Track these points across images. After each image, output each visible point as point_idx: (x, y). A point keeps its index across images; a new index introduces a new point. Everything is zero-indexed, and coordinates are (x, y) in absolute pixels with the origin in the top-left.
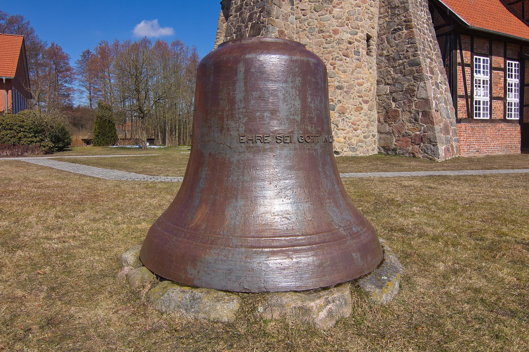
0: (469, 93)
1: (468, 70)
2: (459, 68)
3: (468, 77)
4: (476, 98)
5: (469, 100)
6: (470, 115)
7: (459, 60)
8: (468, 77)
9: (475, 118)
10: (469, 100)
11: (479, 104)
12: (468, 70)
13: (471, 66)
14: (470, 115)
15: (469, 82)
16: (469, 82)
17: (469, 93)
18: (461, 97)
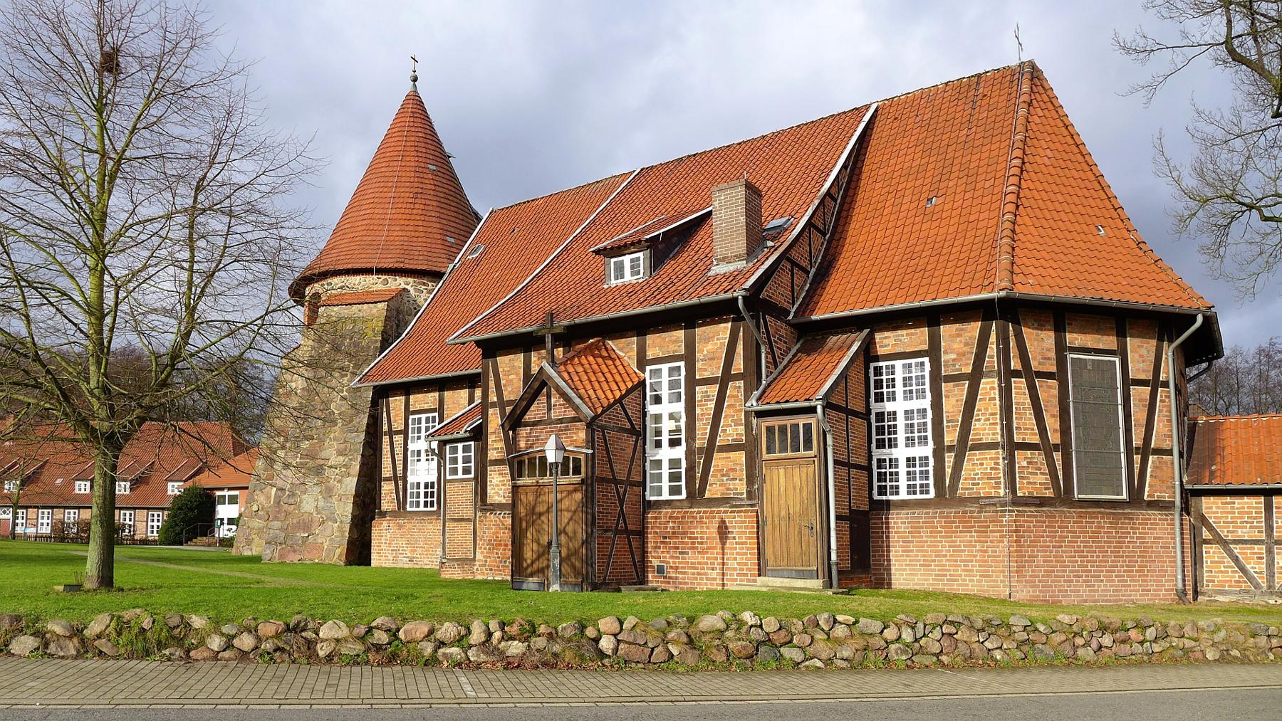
0: (400, 473)
1: (398, 439)
2: (386, 439)
3: (399, 450)
4: (411, 479)
5: (400, 483)
6: (402, 503)
7: (385, 428)
8: (399, 450)
9: (408, 509)
10: (400, 483)
11: (418, 487)
12: (398, 439)
13: (405, 432)
14: (402, 503)
15: (399, 457)
16: (399, 457)
17: (400, 473)
18: (387, 479)
